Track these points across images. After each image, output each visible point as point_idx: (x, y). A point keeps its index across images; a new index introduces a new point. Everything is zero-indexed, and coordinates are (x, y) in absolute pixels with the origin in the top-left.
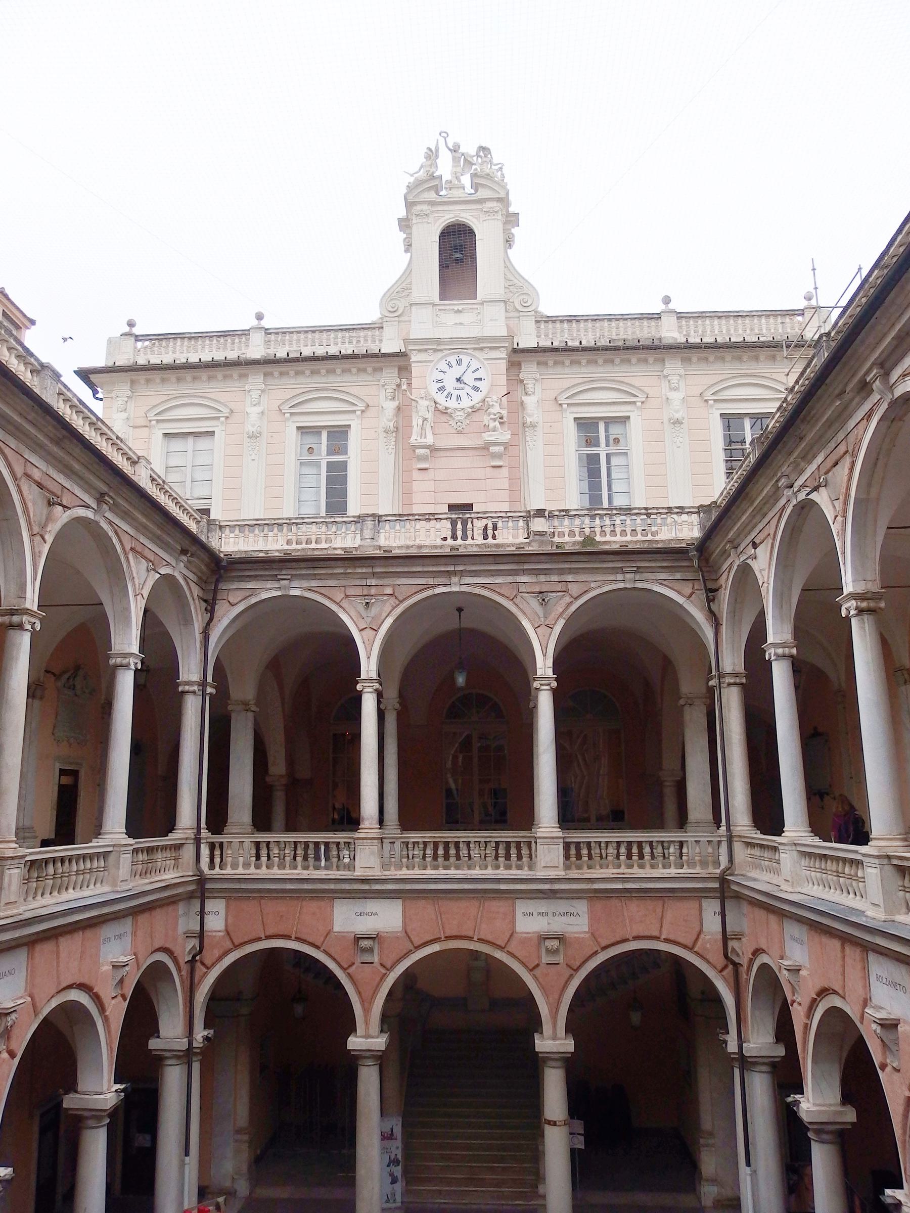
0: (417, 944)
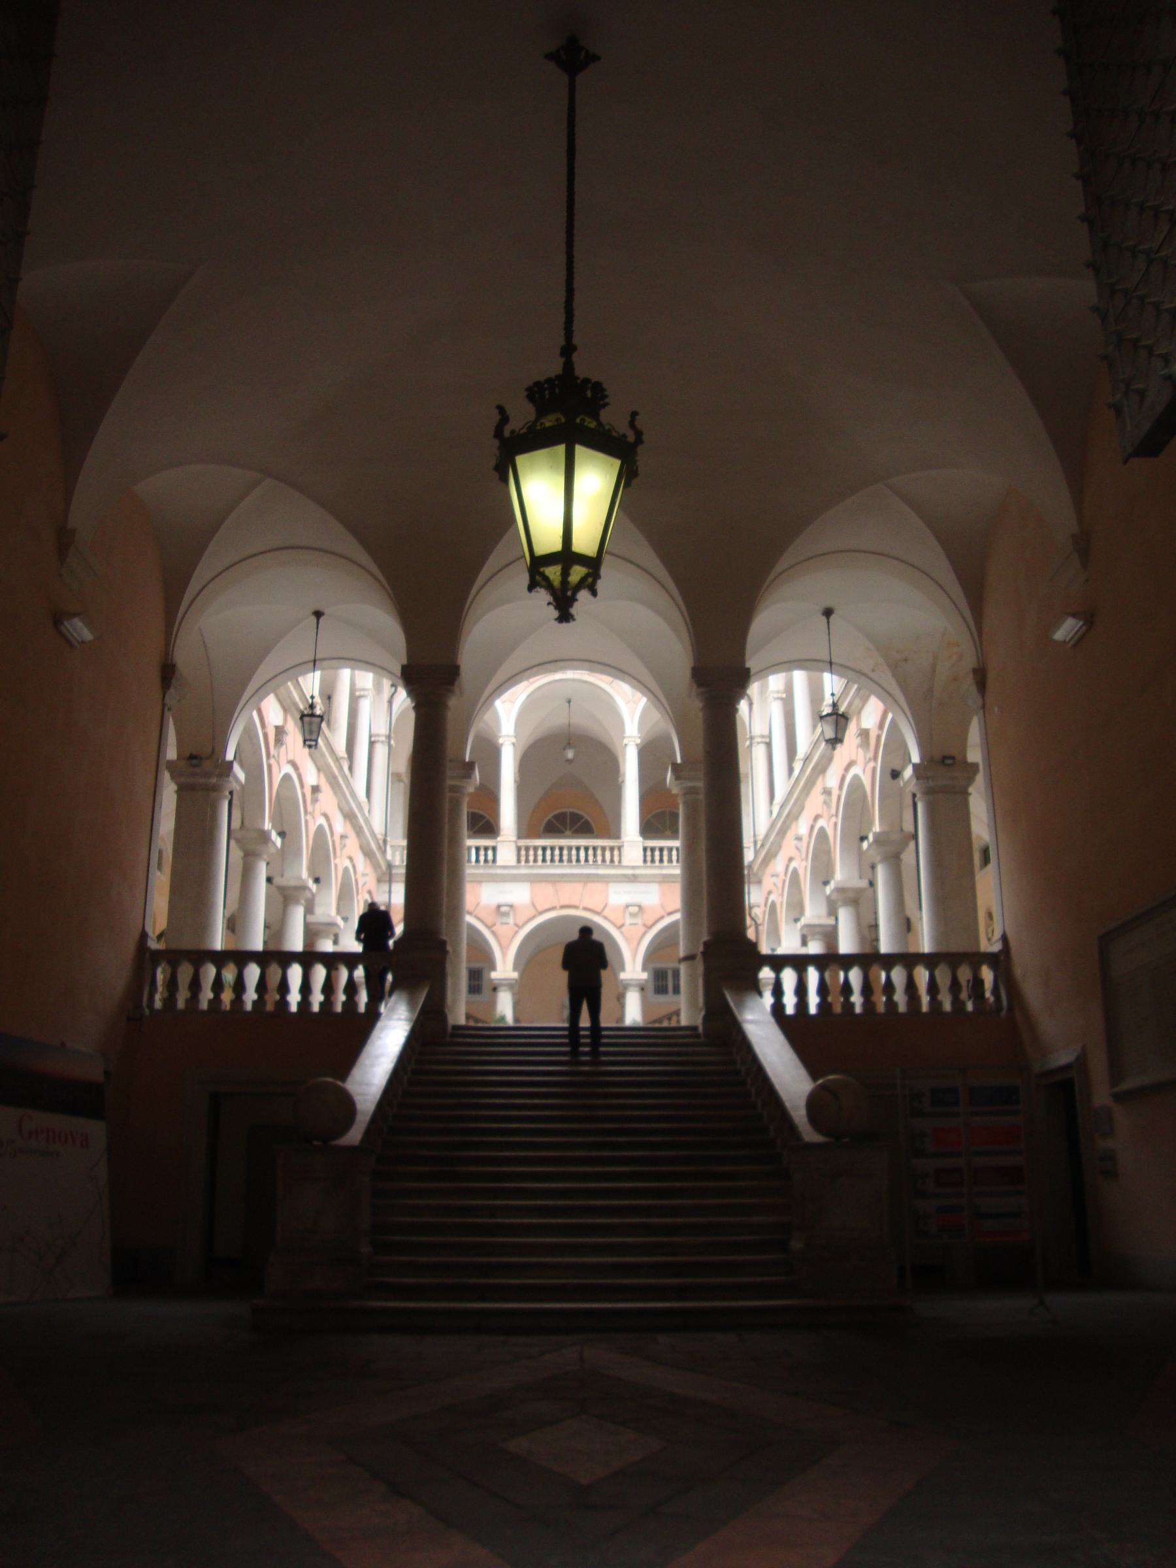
0: (540, 909)
